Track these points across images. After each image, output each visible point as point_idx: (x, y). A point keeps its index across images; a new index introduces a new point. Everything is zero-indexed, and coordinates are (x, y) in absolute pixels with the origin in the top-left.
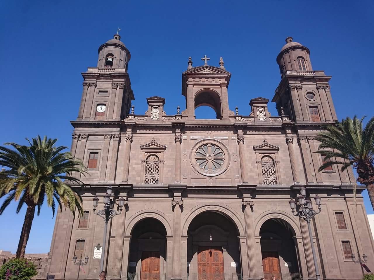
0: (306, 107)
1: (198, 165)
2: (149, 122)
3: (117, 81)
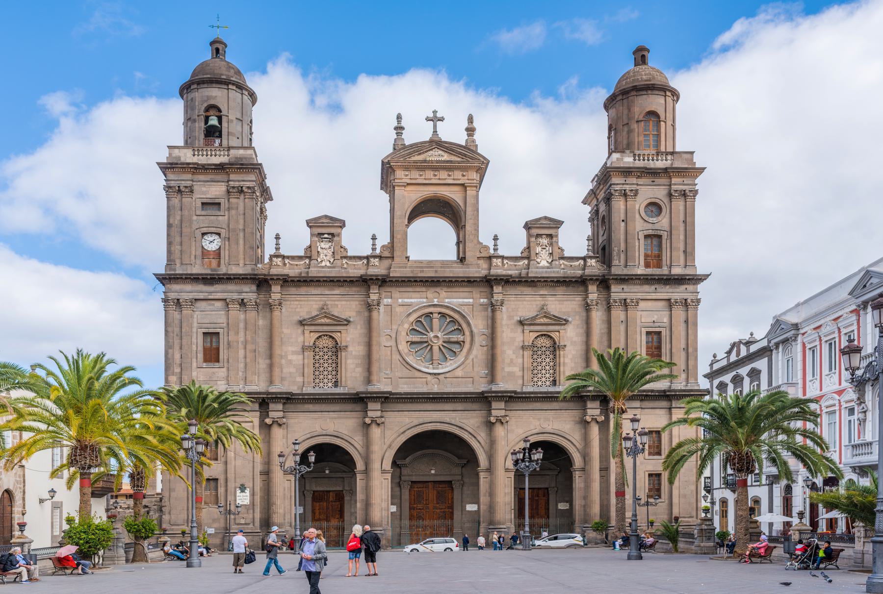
0: (636, 237)
1: (411, 353)
2: (314, 272)
3: (239, 181)
